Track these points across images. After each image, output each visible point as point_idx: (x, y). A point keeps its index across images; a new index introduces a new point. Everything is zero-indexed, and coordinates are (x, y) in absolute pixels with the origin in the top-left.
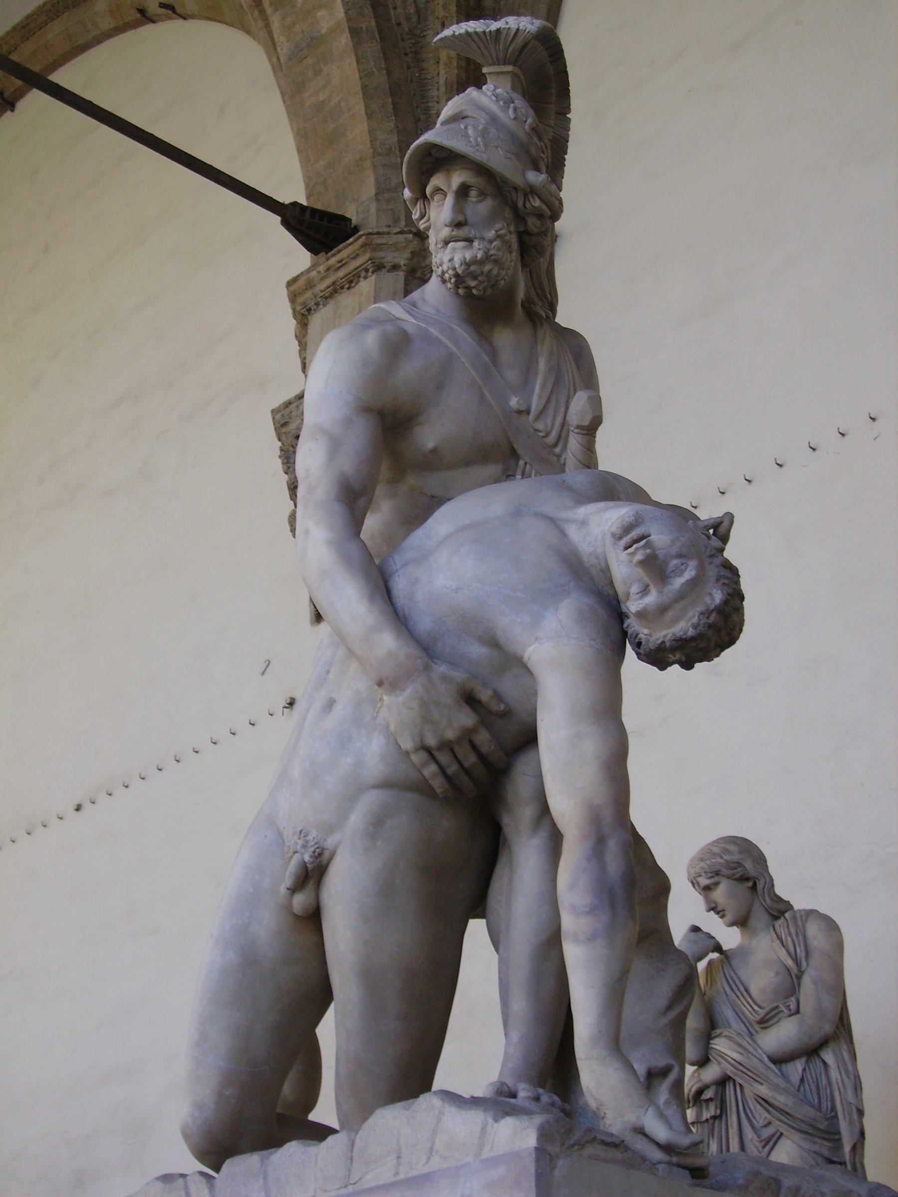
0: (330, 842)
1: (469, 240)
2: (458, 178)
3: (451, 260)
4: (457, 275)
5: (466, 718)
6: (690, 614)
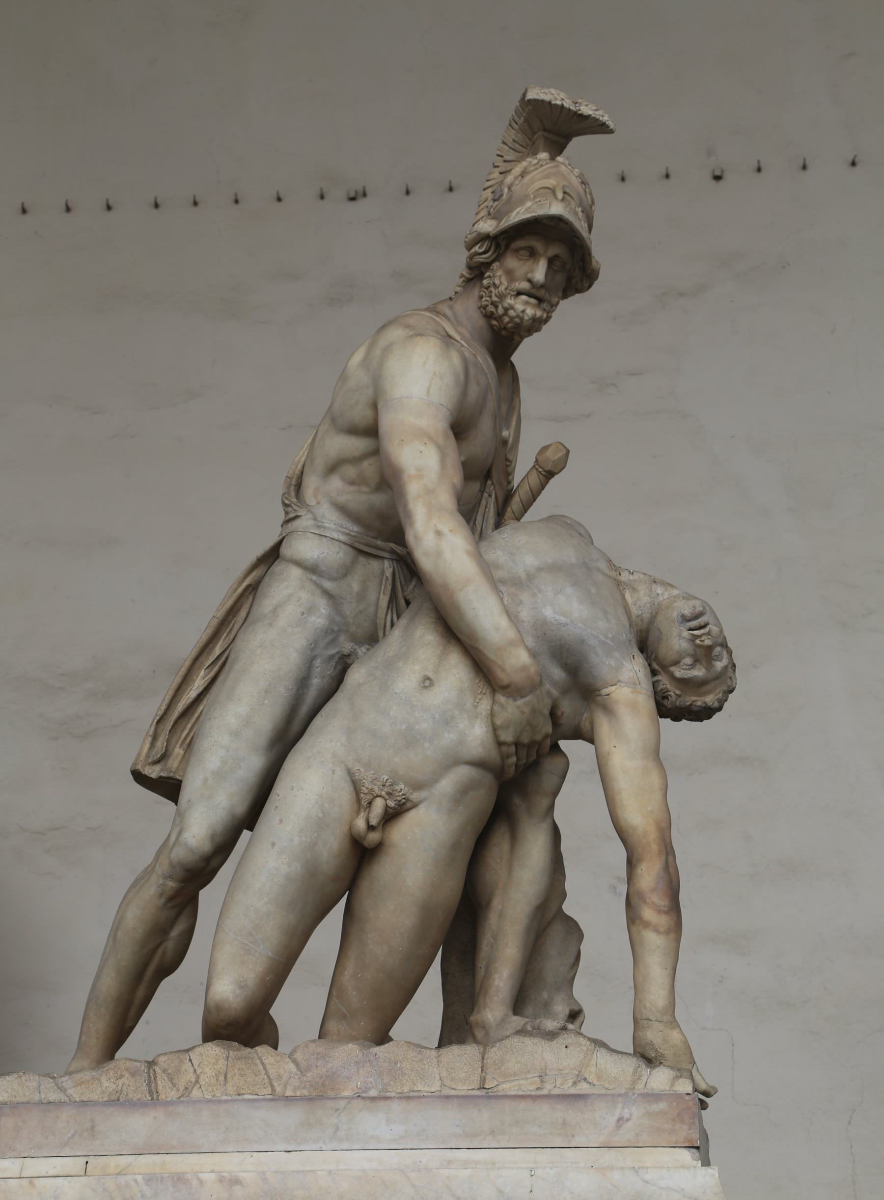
0: (415, 796)
1: (540, 300)
2: (555, 250)
3: (523, 311)
4: (518, 326)
5: (548, 728)
6: (717, 691)
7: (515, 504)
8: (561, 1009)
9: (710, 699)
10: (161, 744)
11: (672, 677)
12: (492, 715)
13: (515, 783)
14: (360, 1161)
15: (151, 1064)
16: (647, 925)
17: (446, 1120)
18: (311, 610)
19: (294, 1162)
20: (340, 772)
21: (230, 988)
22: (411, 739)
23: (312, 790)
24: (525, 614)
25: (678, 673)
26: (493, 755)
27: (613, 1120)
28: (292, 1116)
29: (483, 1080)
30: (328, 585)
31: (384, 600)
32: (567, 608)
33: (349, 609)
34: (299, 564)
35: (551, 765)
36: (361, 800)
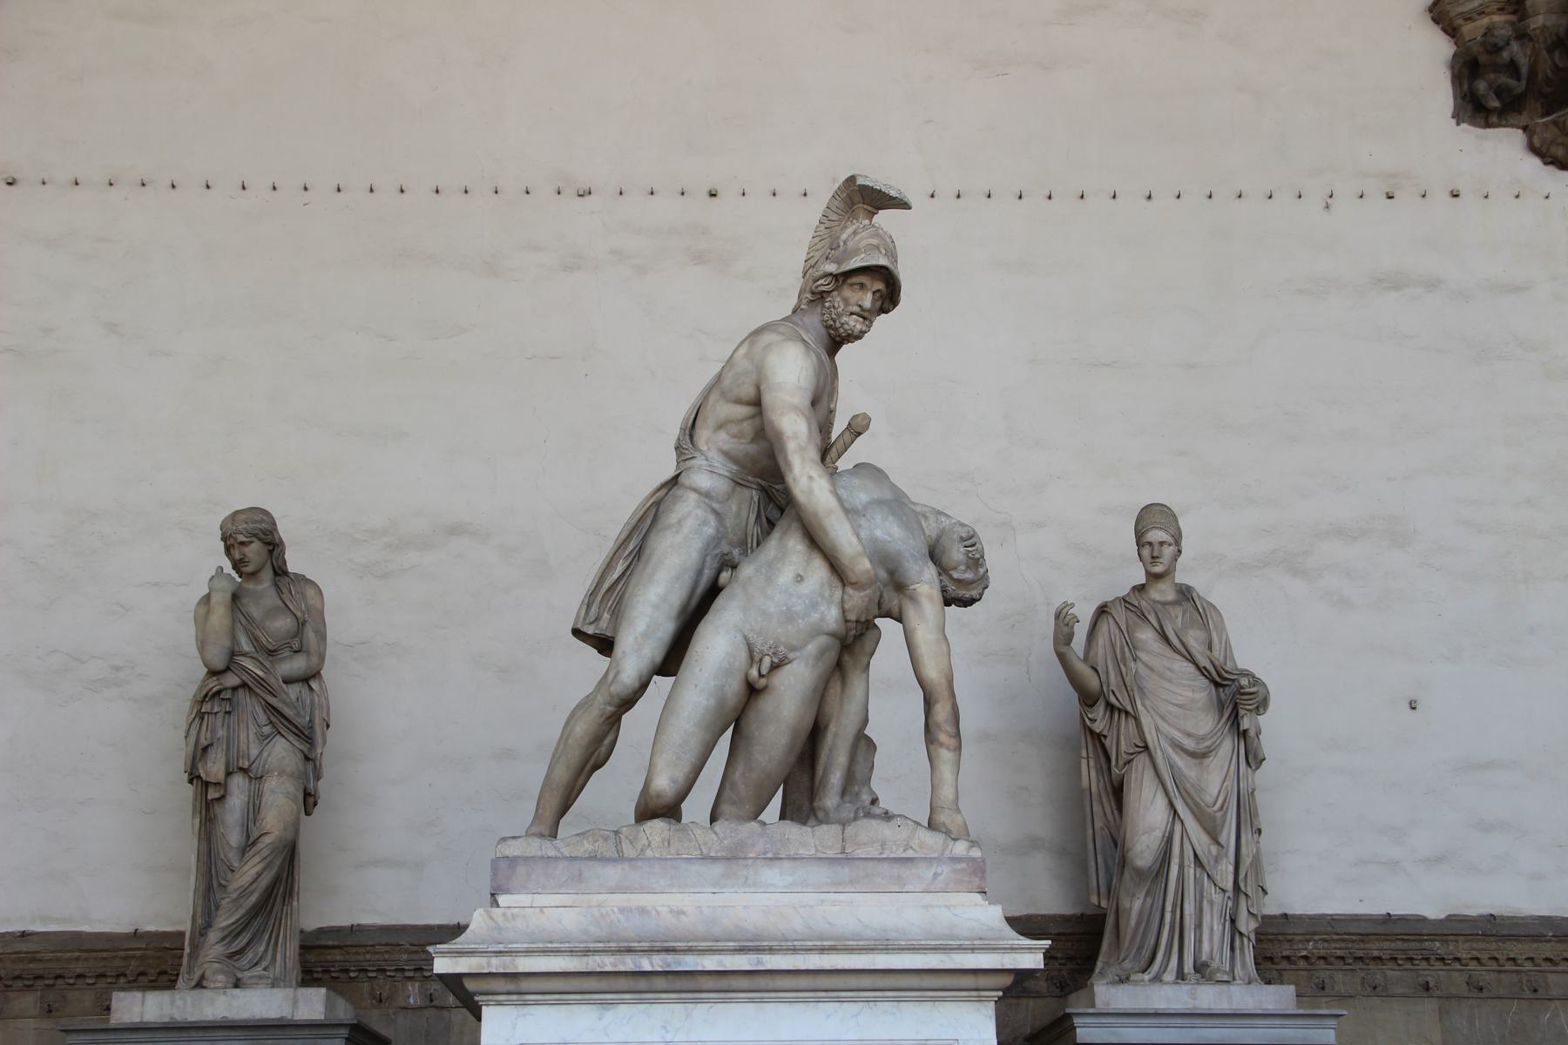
0: (791, 656)
2: (880, 286)
7: (833, 453)
8: (866, 798)
9: (974, 593)
10: (594, 609)
11: (951, 577)
12: (843, 601)
13: (850, 646)
14: (761, 899)
15: (617, 833)
16: (942, 745)
17: (820, 874)
18: (705, 523)
19: (718, 900)
20: (740, 638)
21: (664, 783)
22: (789, 616)
23: (718, 648)
24: (863, 534)
25: (955, 575)
26: (841, 629)
27: (930, 875)
28: (716, 870)
29: (844, 848)
30: (716, 506)
31: (753, 517)
32: (888, 531)
33: (729, 522)
34: (695, 490)
35: (870, 635)
36: (753, 657)
